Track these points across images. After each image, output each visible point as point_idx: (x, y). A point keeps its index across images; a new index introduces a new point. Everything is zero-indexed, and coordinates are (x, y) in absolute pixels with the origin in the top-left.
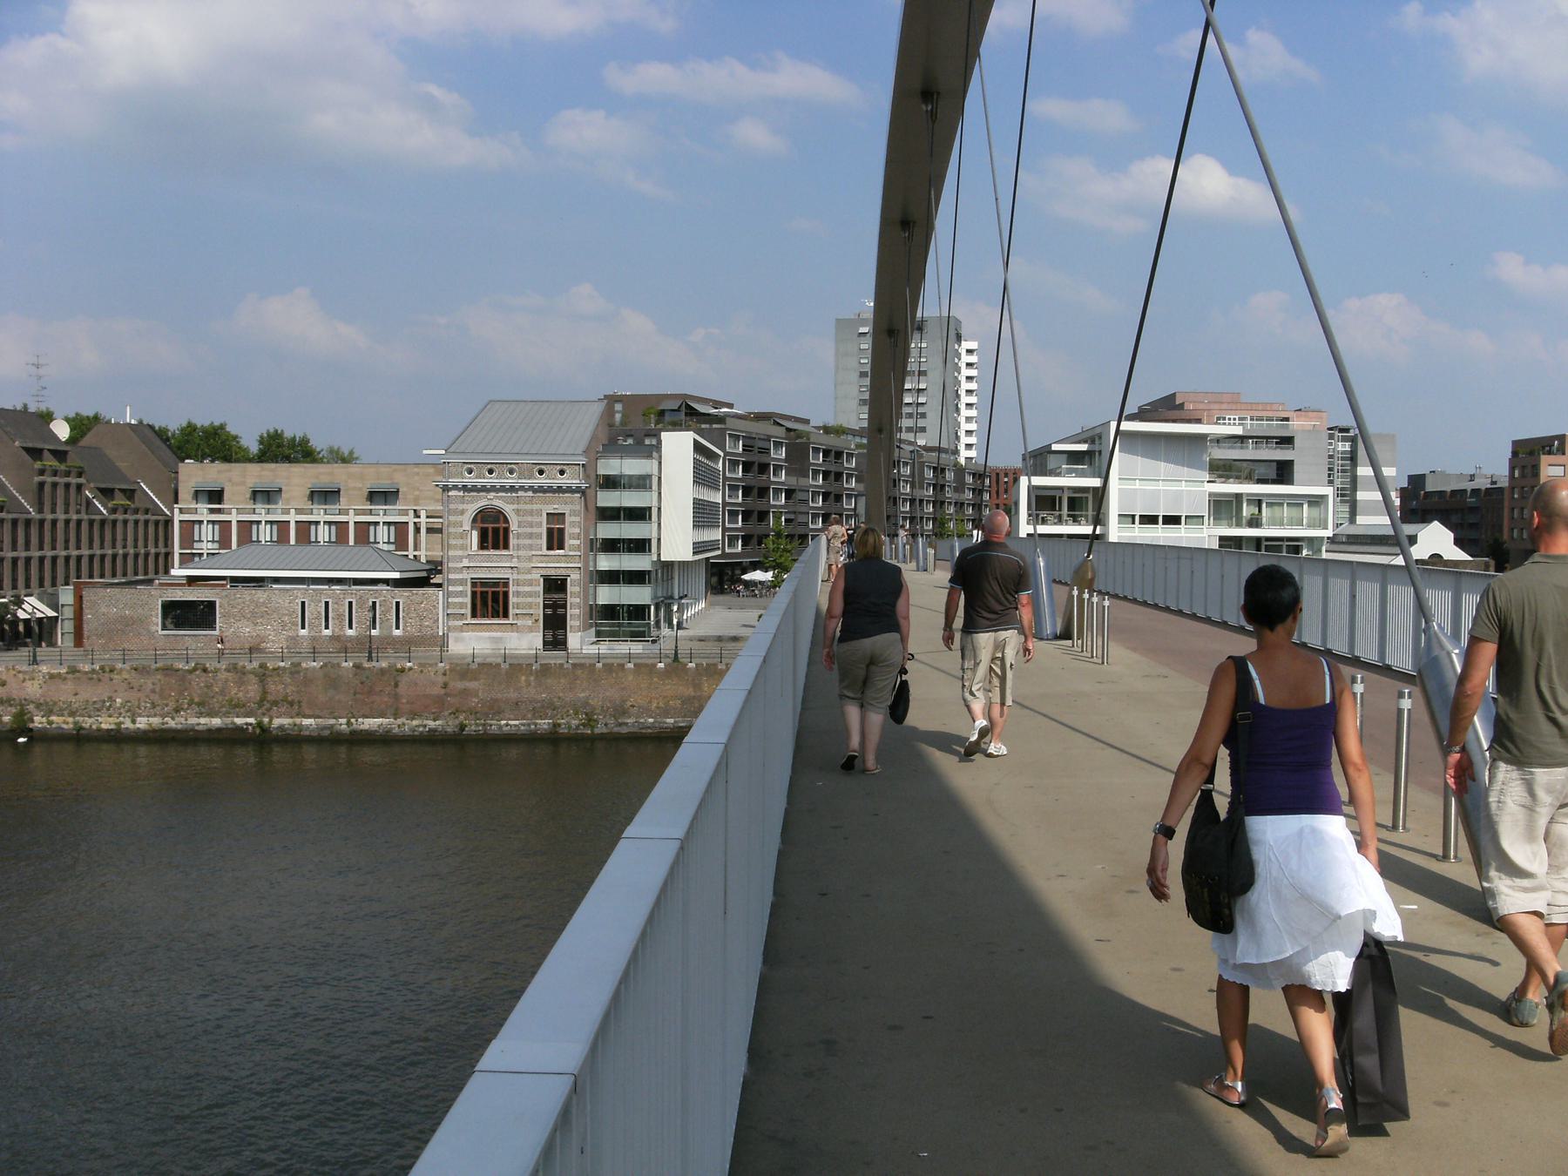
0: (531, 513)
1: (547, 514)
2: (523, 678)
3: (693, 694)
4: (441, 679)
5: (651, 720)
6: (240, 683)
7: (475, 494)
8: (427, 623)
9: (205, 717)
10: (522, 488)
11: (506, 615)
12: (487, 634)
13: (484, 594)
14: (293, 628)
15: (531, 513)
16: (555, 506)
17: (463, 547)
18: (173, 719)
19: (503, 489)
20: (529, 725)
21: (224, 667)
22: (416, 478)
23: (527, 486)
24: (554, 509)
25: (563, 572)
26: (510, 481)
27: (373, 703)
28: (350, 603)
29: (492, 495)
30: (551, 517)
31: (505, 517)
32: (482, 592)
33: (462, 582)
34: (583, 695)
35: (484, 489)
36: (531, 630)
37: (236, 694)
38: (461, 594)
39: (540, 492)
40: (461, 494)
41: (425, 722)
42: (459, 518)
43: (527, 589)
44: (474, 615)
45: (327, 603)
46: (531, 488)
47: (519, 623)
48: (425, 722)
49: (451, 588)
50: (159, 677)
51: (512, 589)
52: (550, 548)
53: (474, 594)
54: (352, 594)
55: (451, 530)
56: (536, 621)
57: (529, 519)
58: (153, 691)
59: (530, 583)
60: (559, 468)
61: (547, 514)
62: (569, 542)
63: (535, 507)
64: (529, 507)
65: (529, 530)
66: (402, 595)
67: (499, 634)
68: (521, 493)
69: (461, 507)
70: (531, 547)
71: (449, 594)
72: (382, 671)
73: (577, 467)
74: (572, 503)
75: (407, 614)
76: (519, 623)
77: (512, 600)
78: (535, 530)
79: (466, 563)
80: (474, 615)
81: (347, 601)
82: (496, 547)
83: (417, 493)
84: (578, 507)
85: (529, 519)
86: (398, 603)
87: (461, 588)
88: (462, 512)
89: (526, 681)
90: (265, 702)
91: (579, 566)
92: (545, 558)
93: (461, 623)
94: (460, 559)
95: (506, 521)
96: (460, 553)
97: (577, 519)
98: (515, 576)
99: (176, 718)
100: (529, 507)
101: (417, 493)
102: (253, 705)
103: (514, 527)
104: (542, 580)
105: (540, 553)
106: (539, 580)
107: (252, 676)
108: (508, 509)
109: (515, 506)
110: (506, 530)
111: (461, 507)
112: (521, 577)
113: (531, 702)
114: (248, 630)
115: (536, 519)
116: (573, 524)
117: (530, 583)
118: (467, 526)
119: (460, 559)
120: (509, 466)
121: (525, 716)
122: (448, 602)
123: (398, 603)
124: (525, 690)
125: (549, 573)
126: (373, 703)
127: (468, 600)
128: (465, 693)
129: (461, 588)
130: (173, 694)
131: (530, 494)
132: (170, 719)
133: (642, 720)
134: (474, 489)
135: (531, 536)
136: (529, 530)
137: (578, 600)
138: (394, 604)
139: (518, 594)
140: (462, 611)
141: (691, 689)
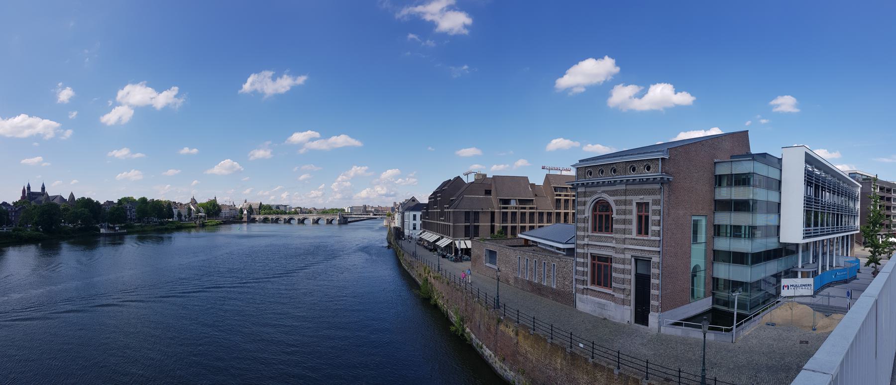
1: (637, 203)
8: (567, 283)
16: (642, 197)
24: (641, 199)
25: (647, 255)
28: (536, 261)
33: (584, 256)
36: (623, 302)
44: (593, 283)
52: (639, 232)
53: (593, 265)
61: (637, 203)
62: (653, 228)
63: (628, 198)
64: (623, 198)
65: (623, 217)
67: (603, 301)
69: (583, 199)
76: (616, 295)
79: (586, 241)
91: (658, 249)
96: (582, 233)
104: (633, 260)
108: (611, 199)
111: (583, 199)
116: (655, 212)
125: (638, 254)
127: (588, 269)
136: (623, 217)
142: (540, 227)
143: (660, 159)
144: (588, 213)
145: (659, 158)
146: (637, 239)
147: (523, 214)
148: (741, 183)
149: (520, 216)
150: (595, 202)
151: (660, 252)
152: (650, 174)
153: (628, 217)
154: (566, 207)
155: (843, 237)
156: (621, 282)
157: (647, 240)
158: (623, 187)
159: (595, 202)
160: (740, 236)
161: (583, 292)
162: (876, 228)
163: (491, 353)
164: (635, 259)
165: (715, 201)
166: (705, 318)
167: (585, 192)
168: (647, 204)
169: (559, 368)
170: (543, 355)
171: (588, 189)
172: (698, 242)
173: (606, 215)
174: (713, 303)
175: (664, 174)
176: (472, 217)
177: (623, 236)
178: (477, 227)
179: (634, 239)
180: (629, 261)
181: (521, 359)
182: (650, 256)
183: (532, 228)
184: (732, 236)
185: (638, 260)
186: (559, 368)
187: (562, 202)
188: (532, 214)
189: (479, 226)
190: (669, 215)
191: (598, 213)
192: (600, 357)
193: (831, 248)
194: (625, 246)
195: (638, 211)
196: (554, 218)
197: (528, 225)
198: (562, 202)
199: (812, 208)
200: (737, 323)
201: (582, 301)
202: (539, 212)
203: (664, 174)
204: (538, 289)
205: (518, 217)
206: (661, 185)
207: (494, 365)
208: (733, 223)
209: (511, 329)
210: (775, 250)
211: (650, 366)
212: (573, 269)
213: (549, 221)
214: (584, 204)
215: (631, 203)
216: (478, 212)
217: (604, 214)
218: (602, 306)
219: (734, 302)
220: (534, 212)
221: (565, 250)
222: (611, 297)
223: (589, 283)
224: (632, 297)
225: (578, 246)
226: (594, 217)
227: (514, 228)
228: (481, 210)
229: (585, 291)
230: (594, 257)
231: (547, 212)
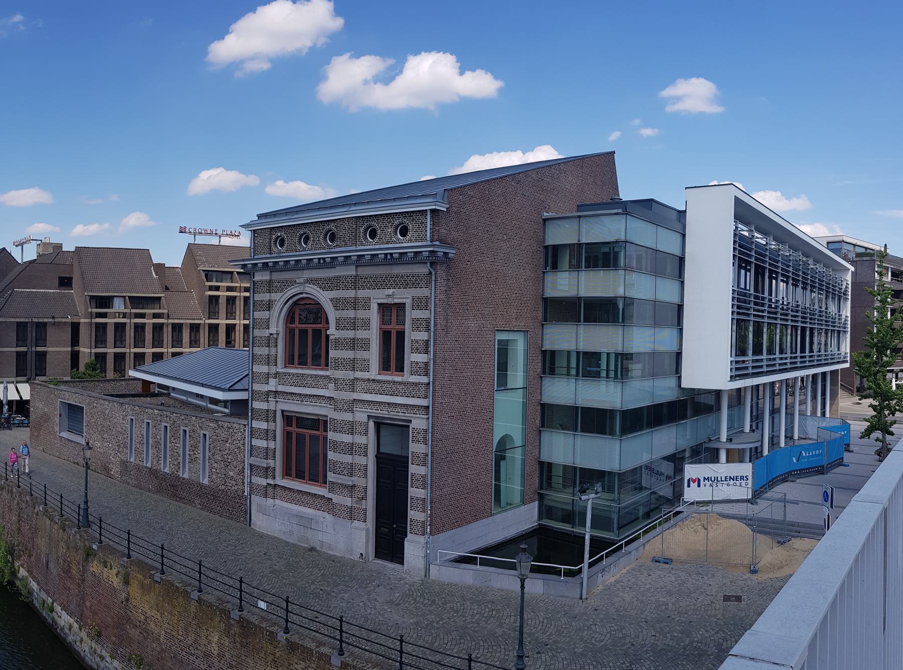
1: (379, 305)
8: (231, 473)
16: (390, 291)
24: (388, 296)
25: (401, 415)
31: (327, 318)
33: (268, 416)
36: (351, 514)
44: (287, 473)
52: (385, 366)
53: (288, 436)
61: (379, 305)
62: (412, 357)
63: (362, 293)
64: (351, 293)
65: (350, 334)
69: (266, 297)
75: (213, 455)
76: (336, 498)
79: (272, 385)
80: (287, 473)
91: (424, 402)
96: (264, 369)
104: (371, 424)
106: (367, 424)
108: (324, 297)
111: (266, 297)
116: (418, 324)
125: (383, 413)
127: (277, 445)
136: (350, 334)
142: (174, 355)
143: (429, 213)
144: (277, 327)
145: (426, 210)
146: (379, 381)
147: (140, 328)
148: (600, 263)
149: (132, 330)
150: (291, 302)
151: (428, 407)
152: (407, 245)
153: (361, 334)
154: (230, 314)
155: (814, 376)
156: (345, 472)
157: (400, 383)
158: (350, 271)
159: (291, 302)
160: (597, 375)
161: (265, 492)
162: (885, 358)
163: (72, 621)
164: (375, 422)
165: (545, 300)
166: (523, 546)
167: (270, 282)
168: (401, 307)
169: (216, 653)
170: (182, 624)
171: (277, 276)
172: (509, 387)
173: (314, 331)
174: (540, 517)
175: (437, 243)
176: (31, 334)
177: (351, 375)
178: (42, 356)
179: (374, 380)
180: (363, 427)
181: (134, 633)
182: (408, 416)
183: (158, 357)
184: (581, 375)
185: (382, 426)
186: (216, 653)
187: (222, 302)
188: (158, 328)
189: (46, 352)
190: (446, 329)
191: (297, 325)
192: (302, 630)
193: (790, 399)
194: (356, 396)
195: (383, 322)
196: (204, 335)
197: (149, 350)
198: (222, 302)
199: (748, 315)
200: (589, 559)
201: (263, 511)
202: (173, 324)
203: (437, 243)
204: (172, 486)
205: (130, 333)
206: (431, 267)
207: (78, 647)
208: (582, 348)
209: (114, 571)
210: (671, 405)
211: (407, 648)
212: (244, 444)
213: (194, 343)
214: (269, 306)
215: (366, 305)
216: (45, 325)
217: (310, 327)
218: (307, 523)
219: (585, 514)
220: (163, 324)
221: (229, 404)
222: (327, 504)
224: (370, 504)
225: (254, 395)
226: (290, 334)
227: (120, 358)
228: (51, 320)
229: (270, 490)
230: (288, 419)
231: (190, 324)
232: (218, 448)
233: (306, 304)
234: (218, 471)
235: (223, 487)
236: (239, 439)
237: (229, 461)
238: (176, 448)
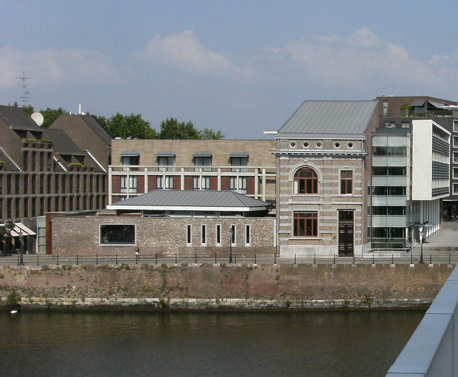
0: (331, 170)
1: (341, 171)
2: (326, 273)
3: (432, 283)
4: (275, 274)
5: (406, 300)
6: (150, 276)
7: (296, 159)
8: (266, 239)
9: (128, 298)
10: (325, 155)
11: (315, 234)
12: (304, 246)
13: (302, 221)
14: (183, 242)
15: (331, 170)
16: (346, 166)
17: (289, 192)
18: (108, 299)
19: (314, 155)
20: (330, 303)
21: (140, 266)
22: (260, 149)
23: (328, 154)
25: (351, 207)
26: (318, 150)
27: (232, 289)
28: (219, 227)
29: (307, 159)
30: (343, 173)
32: (300, 220)
33: (288, 213)
34: (363, 284)
35: (302, 156)
36: (331, 243)
37: (147, 283)
38: (288, 221)
39: (337, 157)
40: (288, 158)
41: (265, 301)
42: (286, 174)
43: (329, 218)
44: (296, 234)
45: (204, 227)
46: (331, 155)
47: (324, 239)
48: (265, 301)
49: (281, 218)
50: (99, 273)
51: (319, 218)
52: (343, 192)
53: (295, 221)
54: (219, 221)
55: (282, 181)
56: (335, 238)
57: (330, 174)
58: (96, 281)
59: (330, 214)
60: (348, 142)
61: (341, 171)
62: (355, 189)
64: (330, 167)
65: (330, 181)
66: (251, 222)
68: (325, 158)
69: (287, 167)
70: (331, 192)
71: (280, 221)
72: (239, 269)
73: (360, 142)
74: (357, 164)
75: (254, 234)
76: (324, 239)
77: (319, 224)
78: (334, 181)
79: (290, 201)
80: (296, 234)
81: (216, 225)
82: (309, 191)
83: (260, 158)
84: (360, 167)
85: (330, 174)
86: (248, 227)
87: (287, 217)
88: (288, 170)
89: (328, 275)
90: (165, 288)
91: (361, 203)
92: (340, 199)
93: (287, 239)
94: (287, 199)
95: (316, 175)
96: (287, 195)
97: (360, 174)
98: (321, 210)
99: (110, 299)
100: (330, 167)
101: (260, 158)
102: (157, 290)
103: (320, 179)
104: (338, 212)
105: (337, 195)
106: (336, 212)
107: (157, 272)
108: (317, 168)
109: (321, 166)
110: (316, 181)
111: (287, 167)
112: (325, 210)
113: (331, 288)
114: (154, 243)
115: (334, 174)
116: (357, 178)
117: (330, 214)
118: (291, 179)
119: (287, 199)
120: (317, 141)
121: (327, 297)
122: (279, 226)
123: (248, 227)
124: (327, 281)
126: (232, 289)
127: (292, 225)
128: (290, 283)
129: (287, 217)
130: (108, 283)
131: (331, 158)
132: (106, 299)
133: (400, 300)
134: (296, 155)
135: (331, 185)
136: (330, 181)
137: (360, 225)
138: (246, 227)
139: (323, 221)
140: (288, 232)
141: (431, 280)
150: (299, 168)
159: (299, 168)
164: (339, 212)
206: (363, 158)
212: (273, 227)
223: (293, 234)
232: (258, 230)
233: (305, 170)
234: (257, 240)
235: (261, 246)
236: (271, 225)
237: (265, 234)
238: (227, 234)
